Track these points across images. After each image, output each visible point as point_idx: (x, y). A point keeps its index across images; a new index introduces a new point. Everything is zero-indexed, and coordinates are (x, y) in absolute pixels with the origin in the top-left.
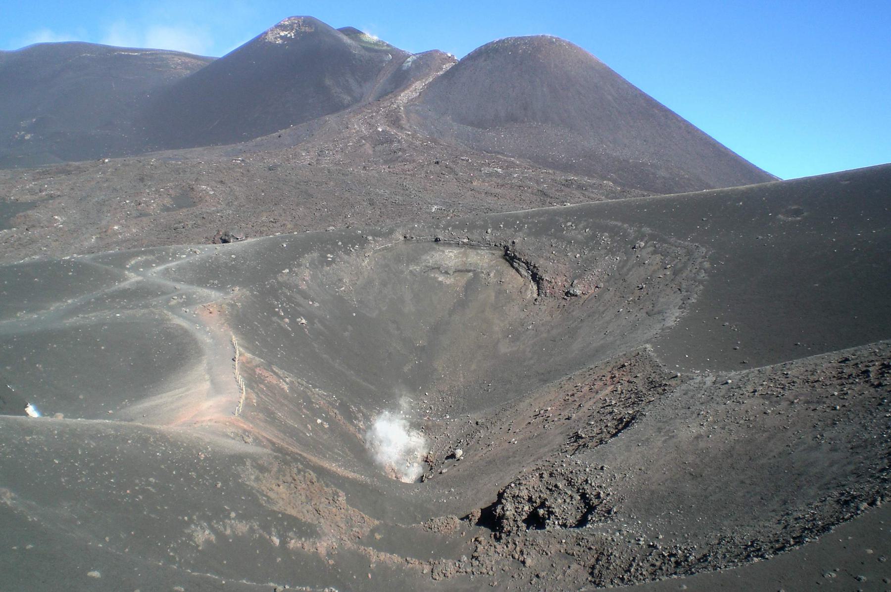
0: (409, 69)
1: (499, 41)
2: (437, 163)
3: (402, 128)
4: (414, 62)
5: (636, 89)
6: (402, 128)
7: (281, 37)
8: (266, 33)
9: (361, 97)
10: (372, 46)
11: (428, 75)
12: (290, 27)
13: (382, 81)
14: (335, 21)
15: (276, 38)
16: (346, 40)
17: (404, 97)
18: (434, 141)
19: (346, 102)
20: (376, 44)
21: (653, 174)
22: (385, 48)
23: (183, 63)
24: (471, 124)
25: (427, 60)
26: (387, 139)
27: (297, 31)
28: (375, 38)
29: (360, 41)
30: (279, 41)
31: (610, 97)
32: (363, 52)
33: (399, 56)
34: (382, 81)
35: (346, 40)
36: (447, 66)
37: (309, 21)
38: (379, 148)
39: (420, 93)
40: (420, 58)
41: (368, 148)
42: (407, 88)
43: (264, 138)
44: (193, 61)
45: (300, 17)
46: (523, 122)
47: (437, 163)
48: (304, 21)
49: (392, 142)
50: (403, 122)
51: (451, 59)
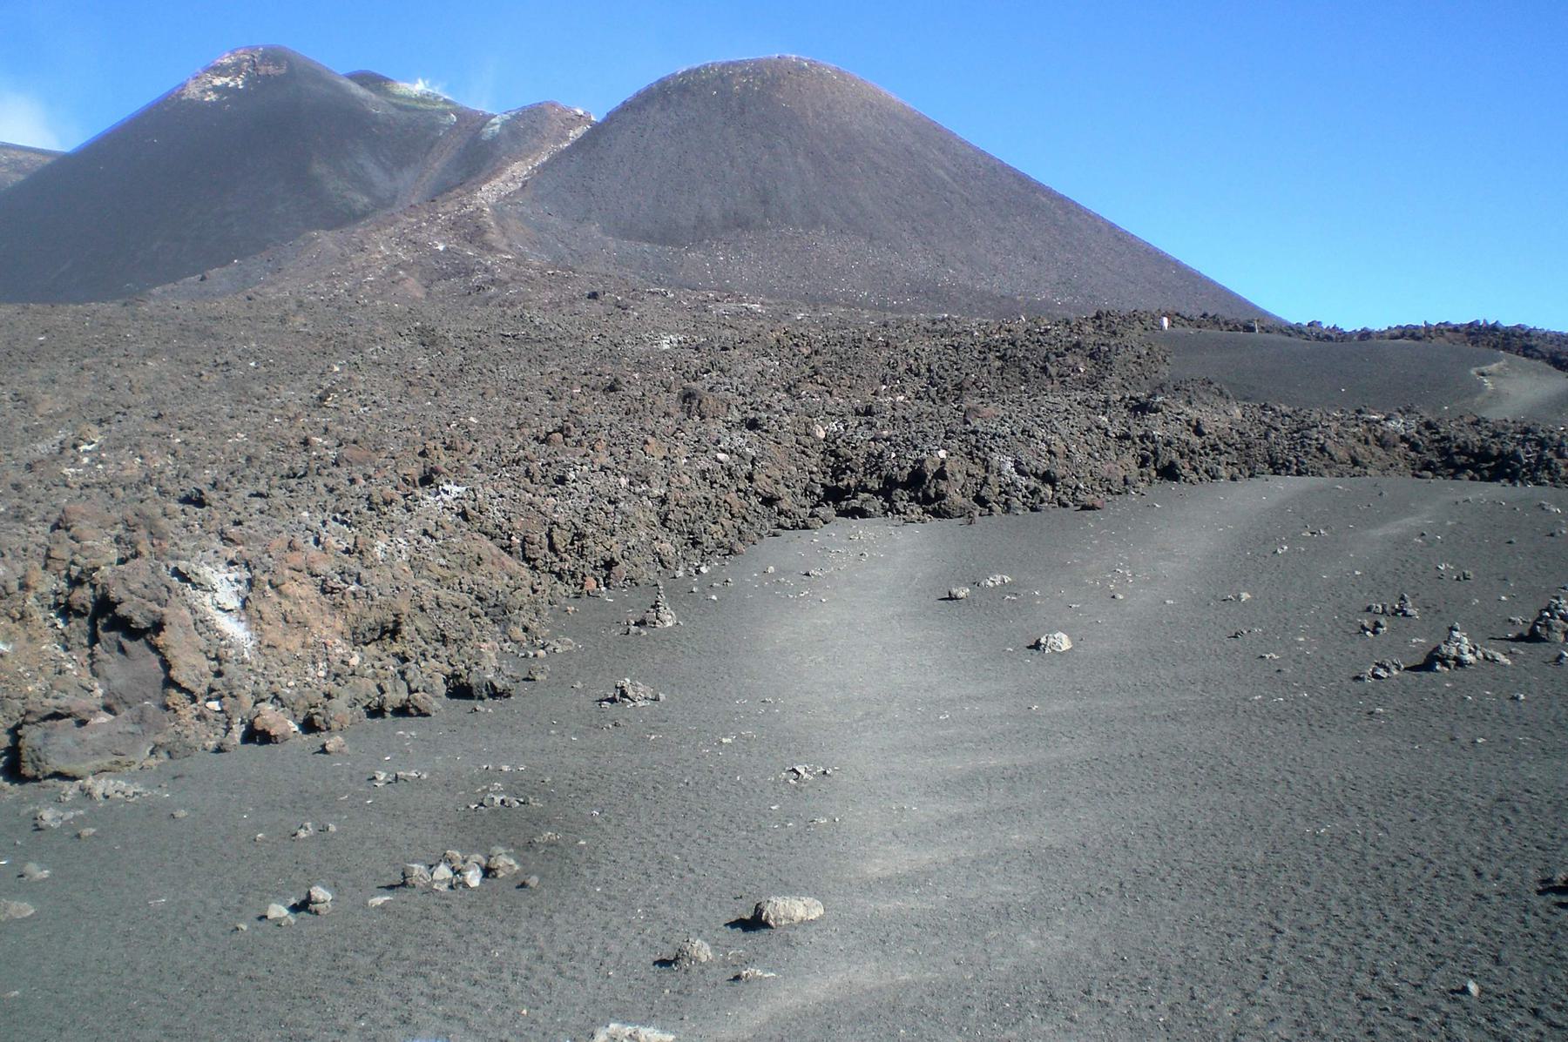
0: (496, 139)
1: (689, 72)
2: (594, 296)
3: (491, 249)
4: (505, 124)
5: (991, 158)
6: (491, 249)
7: (216, 89)
8: (184, 86)
9: (394, 197)
10: (414, 104)
11: (536, 149)
12: (237, 69)
13: (437, 164)
15: (204, 91)
17: (488, 193)
19: (359, 206)
20: (417, 100)
22: (440, 106)
23: (11, 161)
24: (648, 237)
25: (529, 124)
28: (419, 87)
29: (388, 94)
30: (212, 97)
31: (941, 173)
32: (393, 111)
34: (437, 164)
36: (576, 133)
37: (274, 56)
39: (525, 184)
40: (517, 117)
42: (496, 172)
44: (34, 157)
45: (256, 48)
46: (764, 228)
47: (594, 296)
48: (264, 56)
49: (469, 273)
50: (493, 236)
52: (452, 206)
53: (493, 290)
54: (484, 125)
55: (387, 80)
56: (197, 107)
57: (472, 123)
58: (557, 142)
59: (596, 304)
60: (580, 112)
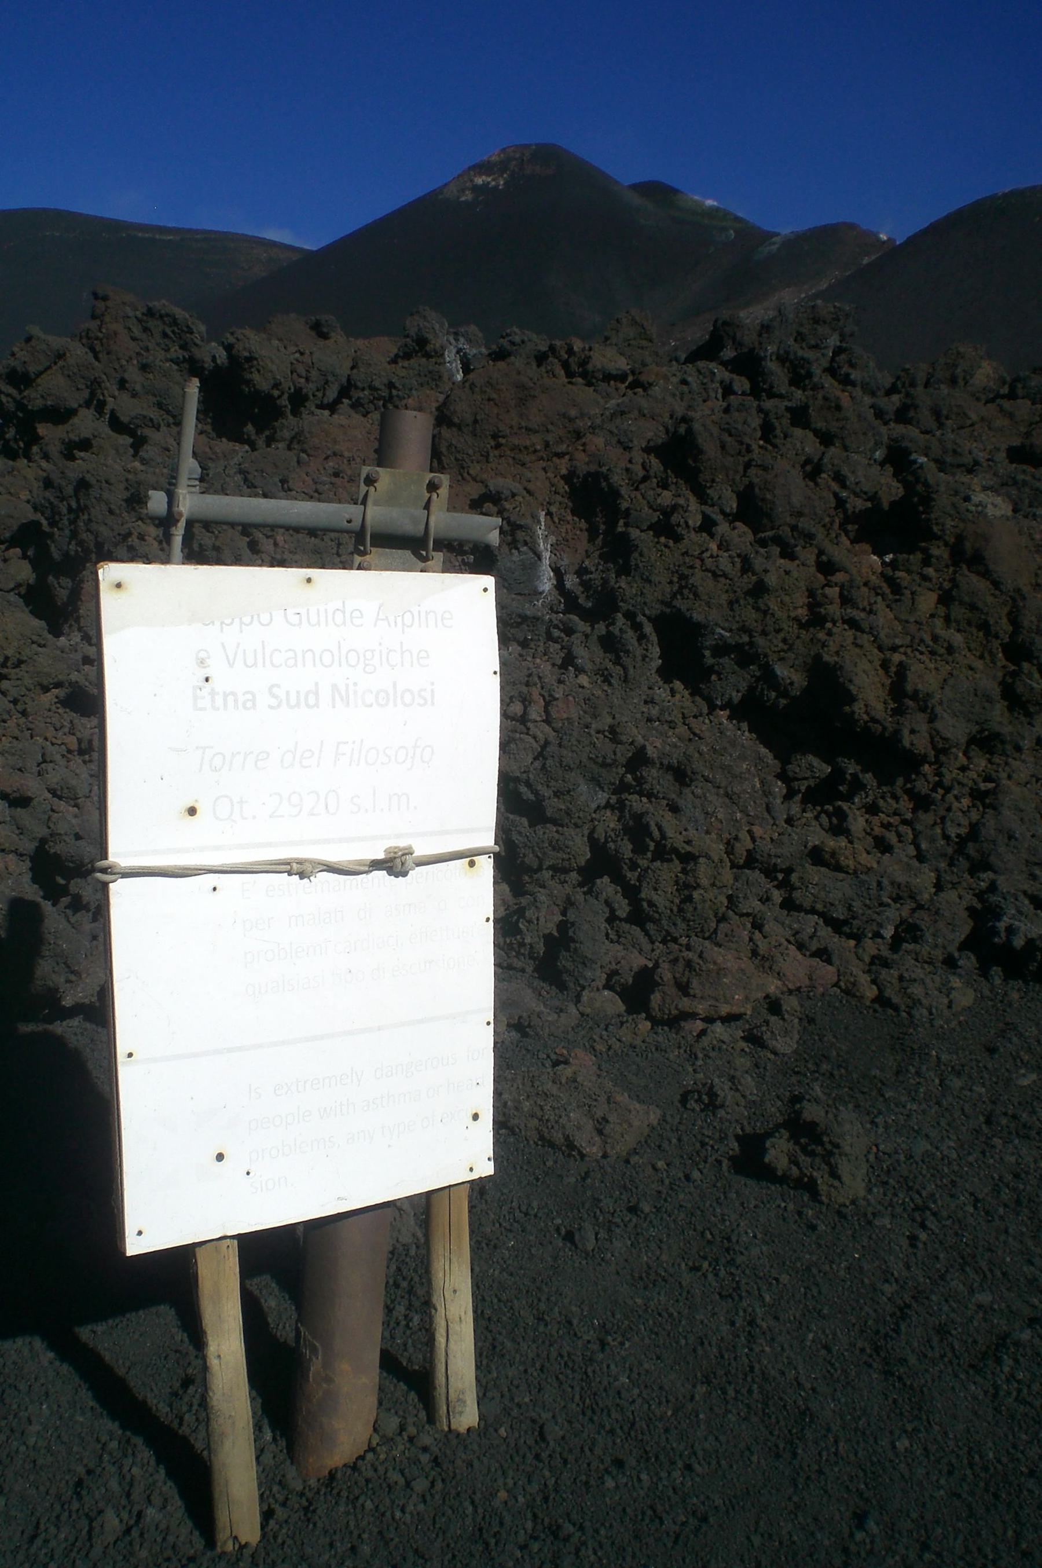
7: (475, 189)
15: (463, 191)
28: (710, 202)
30: (468, 196)
37: (547, 154)
45: (527, 146)
55: (675, 191)
60: (883, 237)
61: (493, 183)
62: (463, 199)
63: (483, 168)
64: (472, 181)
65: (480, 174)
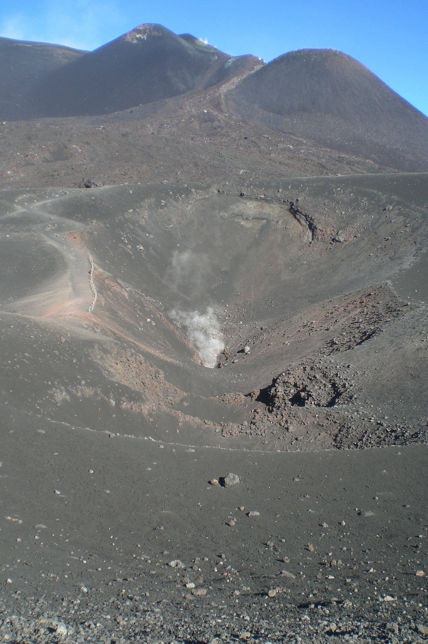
2: (246, 138)
3: (221, 111)
4: (234, 63)
7: (137, 39)
8: (125, 35)
14: (177, 28)
15: (133, 39)
16: (185, 43)
18: (245, 122)
21: (403, 157)
22: (213, 51)
26: (210, 119)
27: (148, 35)
28: (206, 42)
29: (195, 44)
30: (135, 42)
33: (223, 57)
35: (185, 43)
36: (258, 68)
37: (158, 28)
38: (204, 125)
39: (236, 87)
41: (196, 125)
42: (227, 81)
43: (120, 112)
45: (150, 25)
47: (246, 138)
49: (213, 121)
50: (223, 107)
51: (262, 62)
52: (212, 92)
53: (219, 130)
54: (226, 62)
56: (130, 45)
57: (223, 58)
58: (250, 70)
59: (246, 141)
60: (260, 59)
61: (142, 37)
62: (134, 42)
63: (137, 31)
64: (135, 36)
65: (138, 34)
